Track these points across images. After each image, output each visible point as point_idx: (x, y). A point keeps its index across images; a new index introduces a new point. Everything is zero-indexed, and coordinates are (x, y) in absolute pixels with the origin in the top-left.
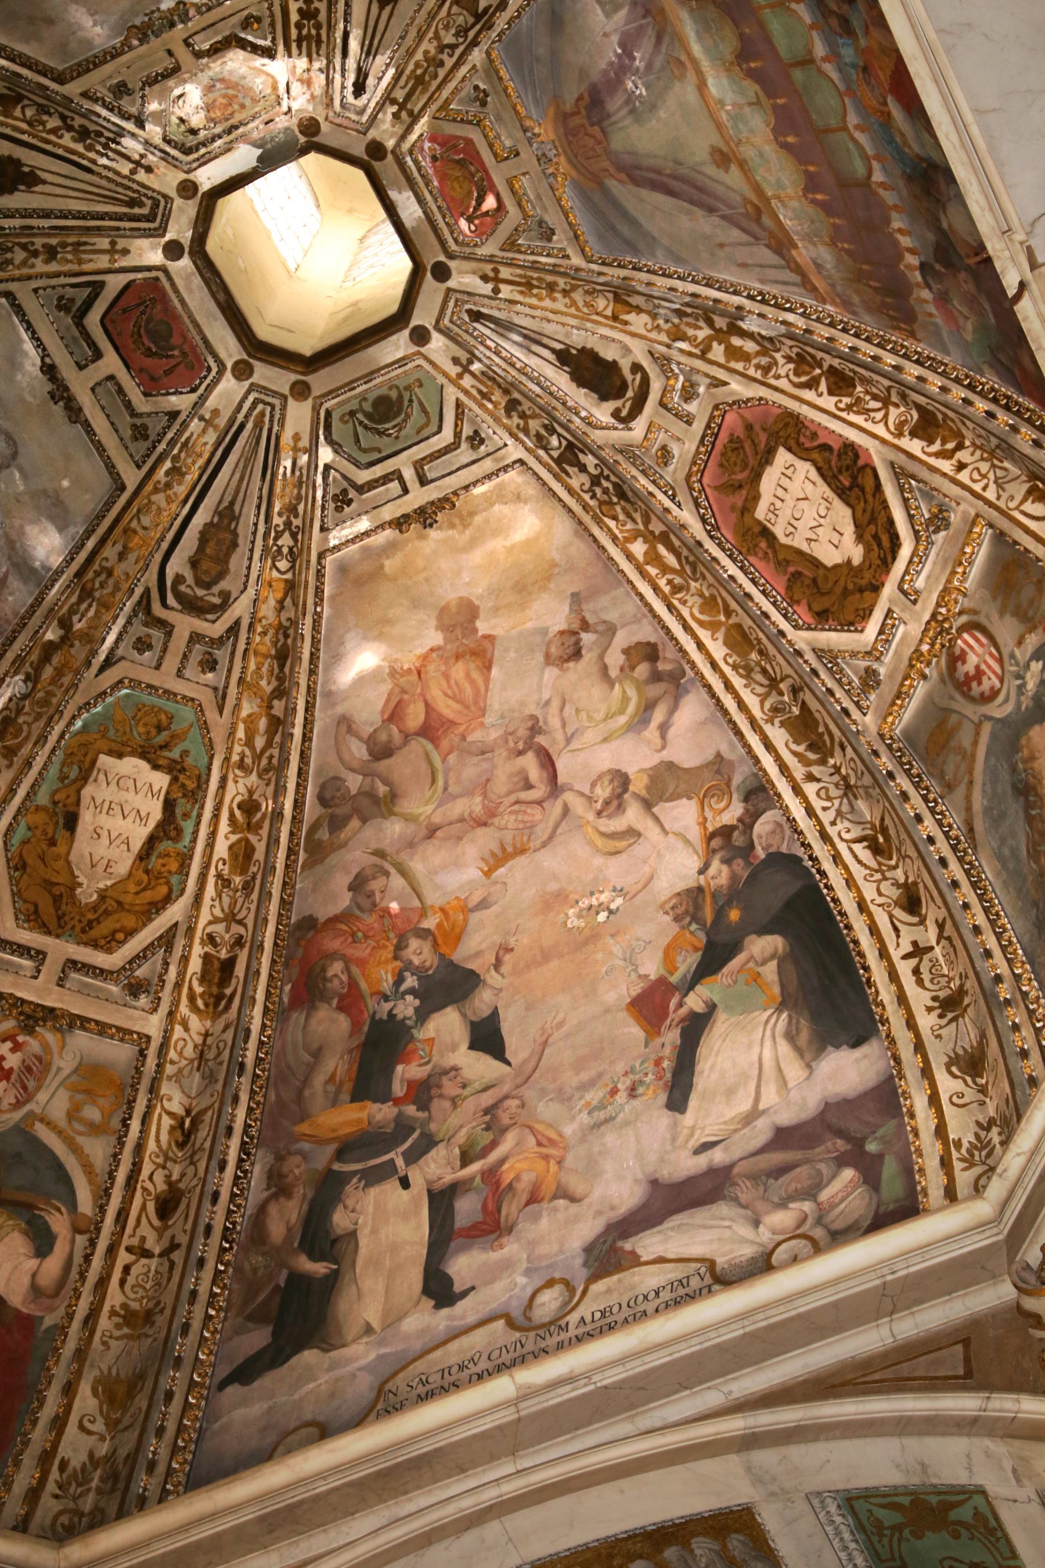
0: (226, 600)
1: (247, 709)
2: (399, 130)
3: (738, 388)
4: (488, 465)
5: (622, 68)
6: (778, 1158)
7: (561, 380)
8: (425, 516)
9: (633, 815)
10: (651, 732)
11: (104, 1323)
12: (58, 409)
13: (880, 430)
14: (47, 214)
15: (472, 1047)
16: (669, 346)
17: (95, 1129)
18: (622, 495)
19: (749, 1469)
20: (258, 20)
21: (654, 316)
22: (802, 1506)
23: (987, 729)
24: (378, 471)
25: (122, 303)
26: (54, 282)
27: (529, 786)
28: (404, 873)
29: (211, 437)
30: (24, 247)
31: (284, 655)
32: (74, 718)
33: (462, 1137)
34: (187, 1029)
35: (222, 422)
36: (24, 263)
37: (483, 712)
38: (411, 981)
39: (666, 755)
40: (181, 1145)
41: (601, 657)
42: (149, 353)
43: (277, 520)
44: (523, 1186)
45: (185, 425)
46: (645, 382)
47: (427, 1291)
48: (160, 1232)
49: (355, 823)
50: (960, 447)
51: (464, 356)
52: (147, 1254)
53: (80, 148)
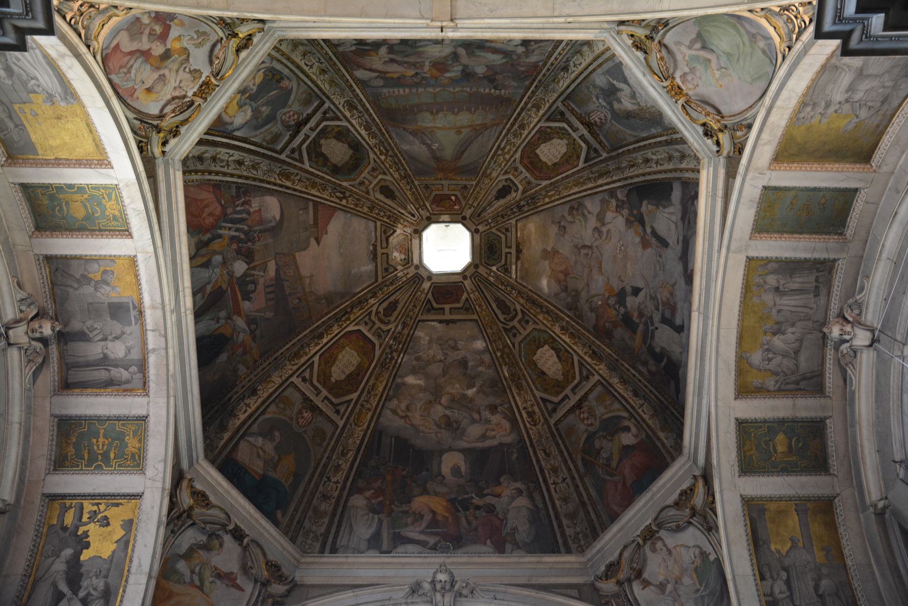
0: (515, 310)
1: (541, 317)
2: (426, 210)
3: (518, 155)
4: (514, 230)
5: (429, 147)
6: (686, 222)
7: (502, 202)
8: (519, 251)
9: (604, 229)
10: (589, 216)
11: (650, 422)
12: (451, 325)
13: (536, 120)
15: (636, 296)
16: (502, 170)
17: (611, 404)
18: (533, 198)
19: (735, 252)
20: (385, 230)
21: (494, 169)
22: (752, 243)
23: (613, 122)
24: (503, 258)
27: (587, 254)
28: (594, 296)
29: (476, 293)
31: (534, 302)
32: (521, 360)
33: (653, 308)
34: (600, 369)
35: (474, 289)
37: (568, 258)
38: (617, 307)
39: (595, 215)
40: (626, 384)
41: (568, 222)
43: (503, 288)
44: (668, 296)
45: (470, 298)
46: (511, 180)
47: (679, 333)
48: (640, 399)
49: (578, 304)
50: (544, 100)
51: (486, 223)
52: (643, 404)
53: (394, 286)
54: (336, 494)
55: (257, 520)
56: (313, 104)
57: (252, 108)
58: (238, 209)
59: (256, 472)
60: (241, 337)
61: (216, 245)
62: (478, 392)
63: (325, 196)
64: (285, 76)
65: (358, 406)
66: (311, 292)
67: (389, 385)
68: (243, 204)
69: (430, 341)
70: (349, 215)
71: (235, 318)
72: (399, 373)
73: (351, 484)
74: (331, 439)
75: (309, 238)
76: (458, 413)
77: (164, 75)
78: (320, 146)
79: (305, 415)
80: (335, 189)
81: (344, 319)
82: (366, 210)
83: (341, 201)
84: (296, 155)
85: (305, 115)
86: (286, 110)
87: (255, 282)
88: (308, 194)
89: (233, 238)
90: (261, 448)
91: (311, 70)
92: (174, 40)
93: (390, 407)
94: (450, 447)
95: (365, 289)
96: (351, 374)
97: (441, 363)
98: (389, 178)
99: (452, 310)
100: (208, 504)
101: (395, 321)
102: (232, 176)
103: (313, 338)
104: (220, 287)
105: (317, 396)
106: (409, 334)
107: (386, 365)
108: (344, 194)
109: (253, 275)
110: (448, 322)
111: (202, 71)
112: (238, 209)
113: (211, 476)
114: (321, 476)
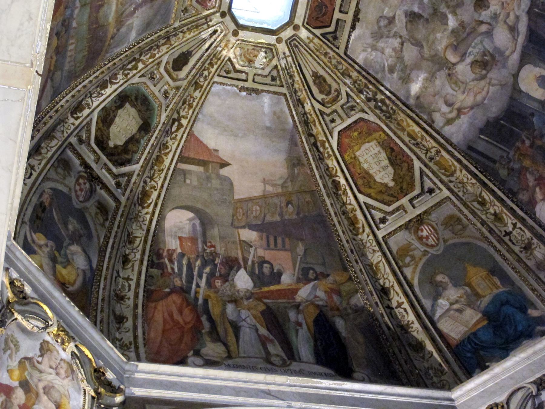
2: (213, 17)
12: (360, 16)
14: (319, 64)
20: (225, 71)
25: (321, 24)
26: (332, 46)
30: (331, 62)
36: (334, 58)
42: (326, 6)
54: (528, 234)
55: (535, 353)
56: (70, 159)
57: (69, 245)
58: (176, 270)
59: (478, 322)
60: (320, 293)
61: (215, 311)
62: (454, 13)
63: (174, 147)
64: (38, 200)
65: (431, 164)
66: (282, 186)
67: (414, 116)
68: (171, 261)
69: (374, 48)
70: (200, 116)
71: (298, 299)
72: (403, 98)
73: (522, 209)
74: (460, 211)
75: (219, 176)
76: (474, 47)
77: (44, 388)
78: (116, 147)
79: (425, 233)
80: (167, 132)
81: (321, 149)
82: (197, 94)
83: (182, 126)
84: (123, 180)
85: (81, 169)
86: (73, 195)
87: (262, 262)
88: (169, 169)
89: (209, 284)
90: (451, 304)
91: (36, 168)
92: (11, 378)
93: (441, 124)
94: (513, 75)
95: (291, 112)
96: (389, 159)
97: (405, 44)
98: (165, 59)
99: (342, 9)
100: (503, 406)
101: (338, 84)
102: (140, 273)
103: (337, 195)
104: (263, 313)
105: (406, 212)
106: (359, 72)
107: (389, 113)
108: (175, 120)
109: (253, 261)
110: (356, 19)
111: (41, 341)
112: (176, 270)
113: (472, 390)
114: (501, 241)
